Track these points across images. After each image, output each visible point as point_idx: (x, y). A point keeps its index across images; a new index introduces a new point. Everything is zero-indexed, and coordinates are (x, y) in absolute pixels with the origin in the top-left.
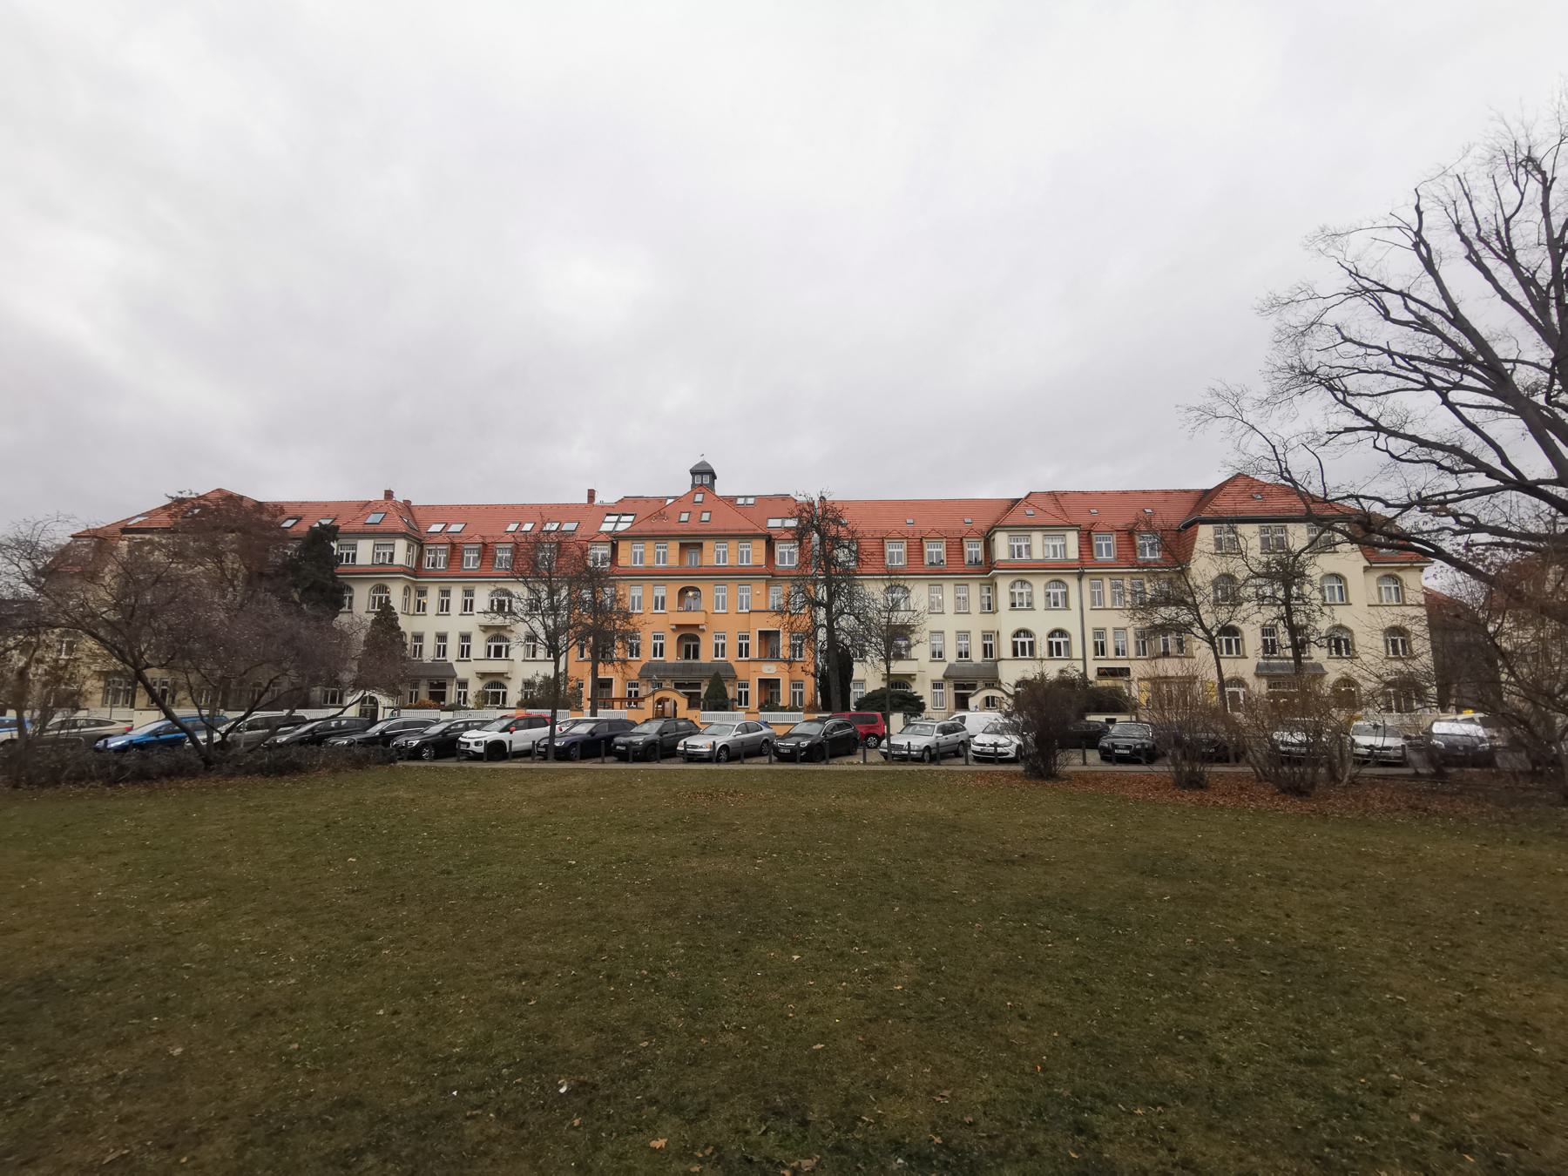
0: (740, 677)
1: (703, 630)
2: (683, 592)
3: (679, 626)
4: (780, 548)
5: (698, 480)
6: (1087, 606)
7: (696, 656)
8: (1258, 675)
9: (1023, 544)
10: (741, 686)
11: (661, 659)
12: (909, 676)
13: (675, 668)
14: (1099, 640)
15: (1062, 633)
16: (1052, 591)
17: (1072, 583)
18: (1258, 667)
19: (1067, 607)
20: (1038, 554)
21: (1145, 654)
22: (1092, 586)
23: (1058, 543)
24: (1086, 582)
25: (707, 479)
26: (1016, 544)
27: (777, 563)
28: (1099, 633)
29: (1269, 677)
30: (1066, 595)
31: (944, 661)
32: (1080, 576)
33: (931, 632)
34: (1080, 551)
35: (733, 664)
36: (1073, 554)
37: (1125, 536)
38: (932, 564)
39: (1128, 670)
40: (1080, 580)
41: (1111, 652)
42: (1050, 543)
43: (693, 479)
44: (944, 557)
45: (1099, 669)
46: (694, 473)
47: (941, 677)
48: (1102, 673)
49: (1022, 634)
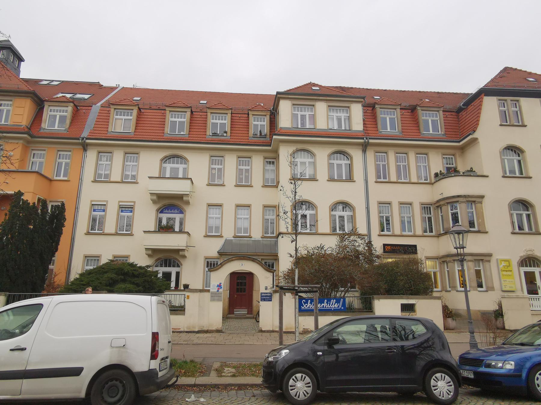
4: (49, 112)
6: (372, 177)
9: (307, 114)
12: (177, 251)
14: (385, 215)
15: (346, 205)
16: (336, 162)
17: (357, 155)
19: (350, 179)
20: (322, 124)
21: (431, 231)
22: (376, 159)
23: (343, 115)
24: (370, 154)
26: (300, 113)
28: (385, 204)
30: (350, 167)
31: (221, 236)
32: (365, 147)
33: (209, 205)
34: (364, 124)
36: (358, 125)
37: (407, 113)
38: (215, 134)
39: (415, 246)
40: (364, 151)
41: (397, 228)
42: (335, 114)
44: (228, 129)
45: (385, 245)
47: (215, 254)
48: (389, 249)
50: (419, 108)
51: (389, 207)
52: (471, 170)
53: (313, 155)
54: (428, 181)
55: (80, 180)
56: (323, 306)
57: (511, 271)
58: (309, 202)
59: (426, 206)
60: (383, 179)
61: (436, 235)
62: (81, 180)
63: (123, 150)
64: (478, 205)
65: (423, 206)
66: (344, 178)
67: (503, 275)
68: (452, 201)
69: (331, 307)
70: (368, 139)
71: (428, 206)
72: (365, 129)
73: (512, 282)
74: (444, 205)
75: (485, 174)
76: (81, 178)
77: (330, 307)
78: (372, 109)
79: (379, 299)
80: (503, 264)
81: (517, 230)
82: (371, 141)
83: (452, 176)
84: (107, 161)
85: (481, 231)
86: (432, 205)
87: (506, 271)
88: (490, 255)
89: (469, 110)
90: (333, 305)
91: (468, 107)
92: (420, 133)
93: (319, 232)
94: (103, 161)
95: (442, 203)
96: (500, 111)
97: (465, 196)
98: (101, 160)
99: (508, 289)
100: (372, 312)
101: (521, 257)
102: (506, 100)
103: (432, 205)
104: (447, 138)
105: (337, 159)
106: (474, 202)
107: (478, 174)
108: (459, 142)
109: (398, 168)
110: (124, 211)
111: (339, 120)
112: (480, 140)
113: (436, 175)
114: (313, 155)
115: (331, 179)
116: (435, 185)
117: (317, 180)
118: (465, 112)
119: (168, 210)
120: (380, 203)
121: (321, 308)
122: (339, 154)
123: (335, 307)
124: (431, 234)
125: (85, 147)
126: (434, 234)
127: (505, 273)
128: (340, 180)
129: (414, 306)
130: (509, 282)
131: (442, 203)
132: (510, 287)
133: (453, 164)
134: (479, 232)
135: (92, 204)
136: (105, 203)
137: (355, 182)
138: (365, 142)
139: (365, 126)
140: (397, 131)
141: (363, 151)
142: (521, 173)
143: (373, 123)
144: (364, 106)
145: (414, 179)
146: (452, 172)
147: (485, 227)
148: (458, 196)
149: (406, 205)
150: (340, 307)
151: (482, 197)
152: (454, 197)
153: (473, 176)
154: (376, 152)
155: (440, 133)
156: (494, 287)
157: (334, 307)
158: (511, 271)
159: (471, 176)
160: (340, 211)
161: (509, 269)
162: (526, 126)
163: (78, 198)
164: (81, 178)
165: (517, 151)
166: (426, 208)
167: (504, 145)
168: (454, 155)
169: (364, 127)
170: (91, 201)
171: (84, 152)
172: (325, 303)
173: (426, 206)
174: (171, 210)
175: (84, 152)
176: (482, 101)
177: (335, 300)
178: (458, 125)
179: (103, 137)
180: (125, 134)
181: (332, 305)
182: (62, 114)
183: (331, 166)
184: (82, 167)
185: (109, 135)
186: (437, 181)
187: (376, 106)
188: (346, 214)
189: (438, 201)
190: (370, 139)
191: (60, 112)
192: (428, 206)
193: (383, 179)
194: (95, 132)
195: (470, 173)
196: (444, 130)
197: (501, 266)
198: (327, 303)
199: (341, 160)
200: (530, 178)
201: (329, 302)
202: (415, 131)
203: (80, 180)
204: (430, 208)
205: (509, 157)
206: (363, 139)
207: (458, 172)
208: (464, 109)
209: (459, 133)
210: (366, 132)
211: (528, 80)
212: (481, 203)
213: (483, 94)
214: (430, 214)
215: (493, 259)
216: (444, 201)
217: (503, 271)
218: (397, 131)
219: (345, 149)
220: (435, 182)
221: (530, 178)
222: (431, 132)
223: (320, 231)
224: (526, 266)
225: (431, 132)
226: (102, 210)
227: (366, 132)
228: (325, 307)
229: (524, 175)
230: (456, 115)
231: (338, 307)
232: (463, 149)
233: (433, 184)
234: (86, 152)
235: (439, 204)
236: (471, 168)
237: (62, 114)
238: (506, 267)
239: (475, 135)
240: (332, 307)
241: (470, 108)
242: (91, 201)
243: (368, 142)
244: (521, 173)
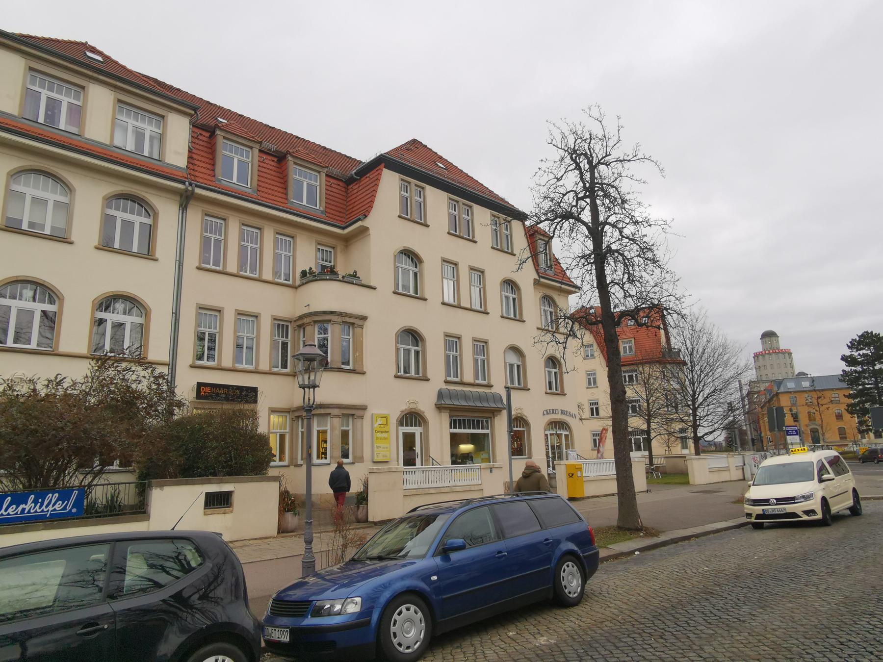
8: (440, 408)
9: (65, 100)
14: (207, 331)
15: (133, 302)
18: (440, 395)
19: (148, 254)
21: (284, 366)
22: (205, 228)
23: (149, 129)
24: (194, 217)
26: (45, 94)
29: (452, 410)
30: (150, 233)
32: (185, 200)
34: (190, 157)
37: (271, 162)
39: (254, 390)
40: (184, 207)
41: (226, 354)
42: (131, 122)
45: (200, 385)
48: (205, 392)
49: (28, 293)
50: (290, 158)
51: (218, 317)
52: (354, 275)
53: (68, 188)
54: (290, 283)
56: (24, 509)
57: (387, 432)
58: (43, 285)
59: (281, 323)
60: (213, 265)
61: (291, 373)
64: (358, 330)
65: (278, 322)
66: (135, 249)
67: (378, 438)
68: (322, 319)
69: (45, 510)
70: (193, 185)
71: (285, 324)
72: (191, 166)
73: (387, 448)
74: (309, 324)
75: (372, 284)
77: (43, 511)
78: (210, 137)
79: (161, 486)
80: (380, 421)
81: (402, 373)
82: (198, 191)
83: (327, 280)
85: (357, 371)
86: (291, 322)
87: (382, 432)
88: (364, 408)
89: (363, 182)
90: (51, 506)
91: (362, 179)
92: (287, 199)
93: (59, 350)
95: (306, 320)
96: (402, 197)
97: (341, 314)
99: (380, 459)
100: (144, 512)
101: (402, 412)
102: (409, 183)
103: (291, 322)
104: (327, 218)
105: (125, 210)
106: (353, 324)
107: (363, 282)
108: (344, 228)
109: (242, 250)
111: (139, 136)
112: (372, 232)
113: (304, 273)
114: (68, 188)
115: (106, 246)
116: (300, 289)
117: (71, 243)
118: (357, 186)
120: (201, 308)
121: (16, 514)
122: (131, 200)
123: (55, 510)
124: (284, 370)
126: (288, 370)
127: (379, 435)
128: (125, 252)
129: (231, 495)
130: (384, 448)
131: (306, 320)
132: (383, 456)
133: (330, 262)
134: (353, 371)
137: (156, 260)
138: (186, 190)
139: (191, 161)
140: (249, 186)
141: (181, 205)
142: (416, 292)
143: (207, 160)
144: (194, 125)
145: (268, 275)
146: (328, 273)
147: (363, 365)
148: (332, 313)
149: (247, 317)
150: (68, 508)
151: (364, 318)
152: (325, 313)
153: (356, 284)
154: (206, 215)
155: (318, 208)
156: (363, 456)
157: (52, 511)
158: (387, 432)
159: (353, 284)
160: (118, 313)
161: (386, 429)
162: (428, 226)
165: (414, 259)
166: (281, 326)
167: (400, 246)
168: (333, 248)
169: (188, 162)
172: (29, 503)
173: (281, 323)
176: (380, 174)
177: (57, 495)
178: (345, 203)
181: (47, 507)
183: (108, 222)
186: (303, 284)
187: (218, 132)
188: (130, 320)
189: (301, 317)
190: (197, 186)
192: (285, 324)
193: (213, 265)
195: (353, 279)
196: (324, 204)
197: (376, 425)
198: (35, 502)
199: (132, 212)
200: (425, 300)
201: (40, 500)
202: (280, 195)
204: (287, 326)
205: (404, 266)
206: (183, 183)
207: (336, 274)
208: (356, 180)
209: (344, 215)
210: (192, 172)
211: (437, 165)
212: (362, 327)
213: (383, 165)
214: (287, 337)
215: (368, 415)
216: (310, 318)
217: (378, 432)
218: (249, 186)
219: (144, 194)
220: (300, 286)
221: (425, 300)
222: (305, 203)
223: (63, 348)
224: (407, 425)
225: (305, 203)
227: (192, 172)
228: (29, 512)
229: (418, 295)
230: (345, 187)
231: (65, 508)
232: (347, 241)
233: (296, 288)
235: (302, 322)
236: (355, 272)
238: (382, 426)
239: (366, 223)
240: (48, 511)
241: (365, 180)
243: (193, 191)
244: (416, 292)
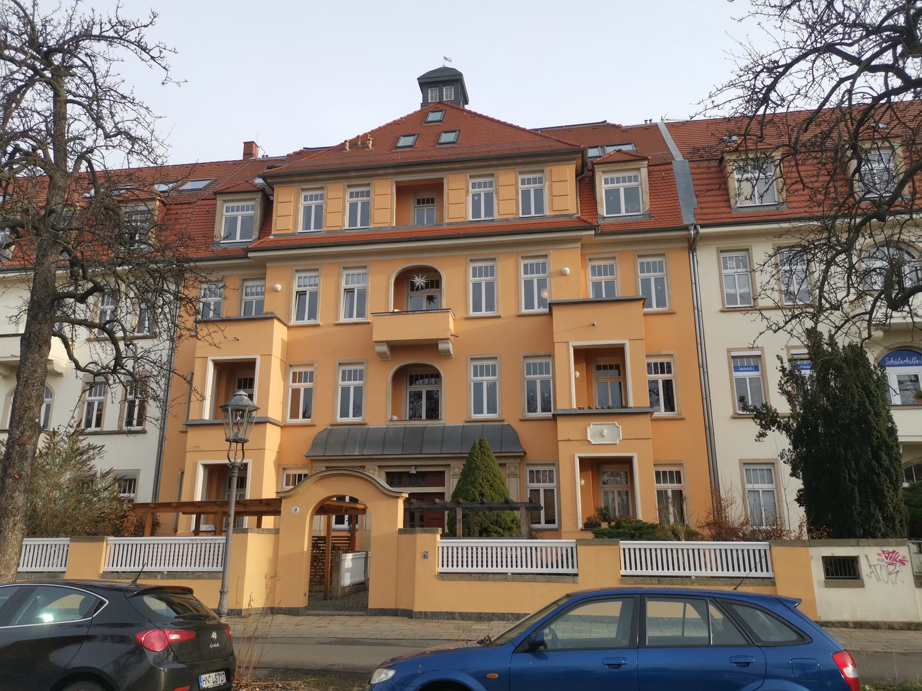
0: (532, 456)
1: (447, 354)
2: (404, 280)
3: (397, 347)
5: (433, 95)
7: (433, 413)
10: (535, 476)
11: (358, 420)
13: (385, 438)
25: (448, 94)
27: (603, 210)
35: (520, 428)
43: (425, 98)
46: (427, 82)
55: (696, 311)
62: (697, 309)
63: (772, 243)
76: (696, 305)
84: (738, 267)
94: (730, 268)
98: (726, 268)
110: (742, 369)
119: (895, 358)
125: (692, 246)
135: (733, 357)
136: (758, 353)
163: (699, 346)
164: (696, 305)
170: (729, 351)
171: (691, 255)
174: (903, 359)
175: (691, 255)
179: (711, 222)
180: (767, 208)
182: (627, 184)
184: (694, 283)
185: (734, 214)
191: (624, 181)
194: (705, 211)
203: (696, 311)
226: (752, 367)
234: (695, 254)
237: (627, 184)
242: (729, 351)
